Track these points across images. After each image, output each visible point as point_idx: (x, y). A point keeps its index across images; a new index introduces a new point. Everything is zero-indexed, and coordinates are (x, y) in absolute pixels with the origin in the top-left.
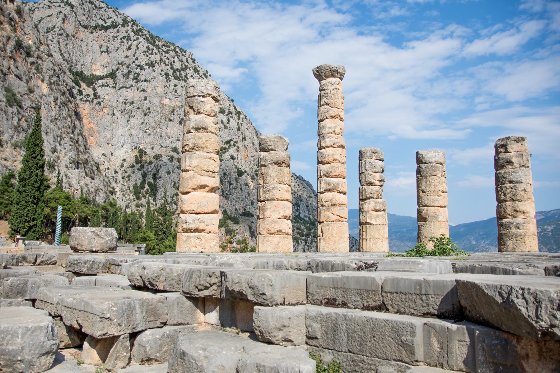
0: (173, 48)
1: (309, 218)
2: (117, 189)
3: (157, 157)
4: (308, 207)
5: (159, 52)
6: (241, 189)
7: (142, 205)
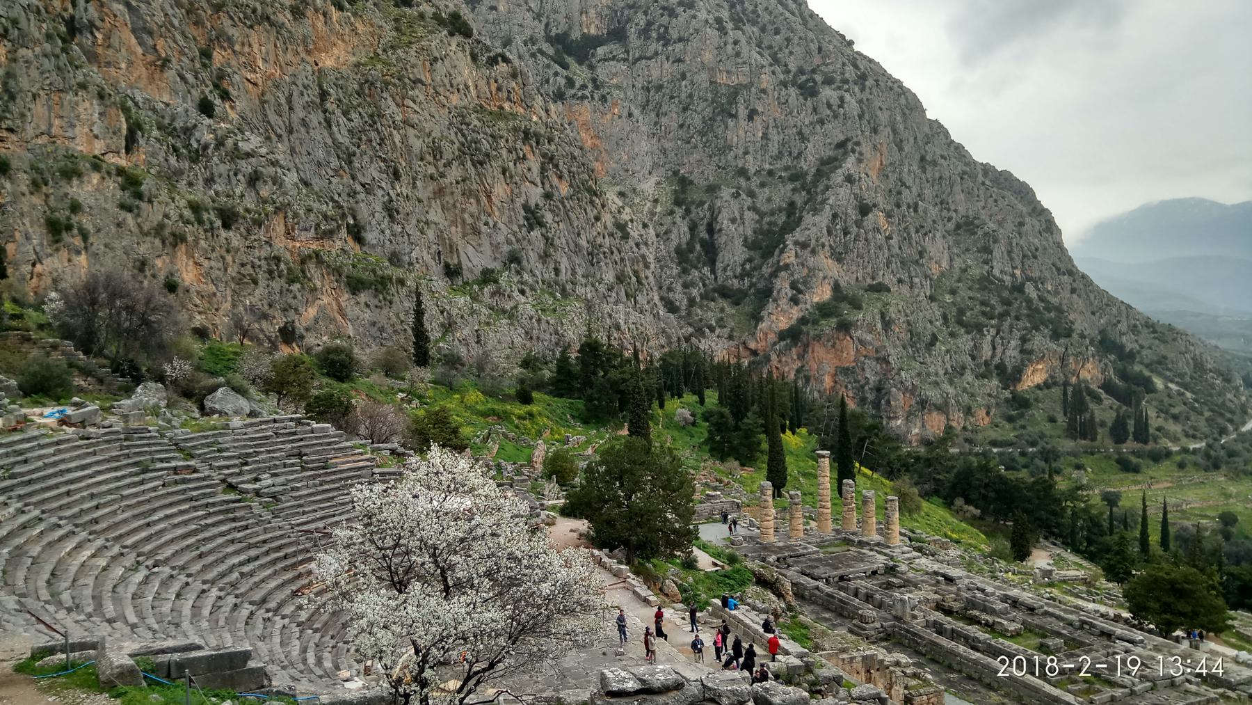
1: (1013, 275)
2: (651, 259)
3: (712, 189)
4: (1010, 252)
6: (866, 240)
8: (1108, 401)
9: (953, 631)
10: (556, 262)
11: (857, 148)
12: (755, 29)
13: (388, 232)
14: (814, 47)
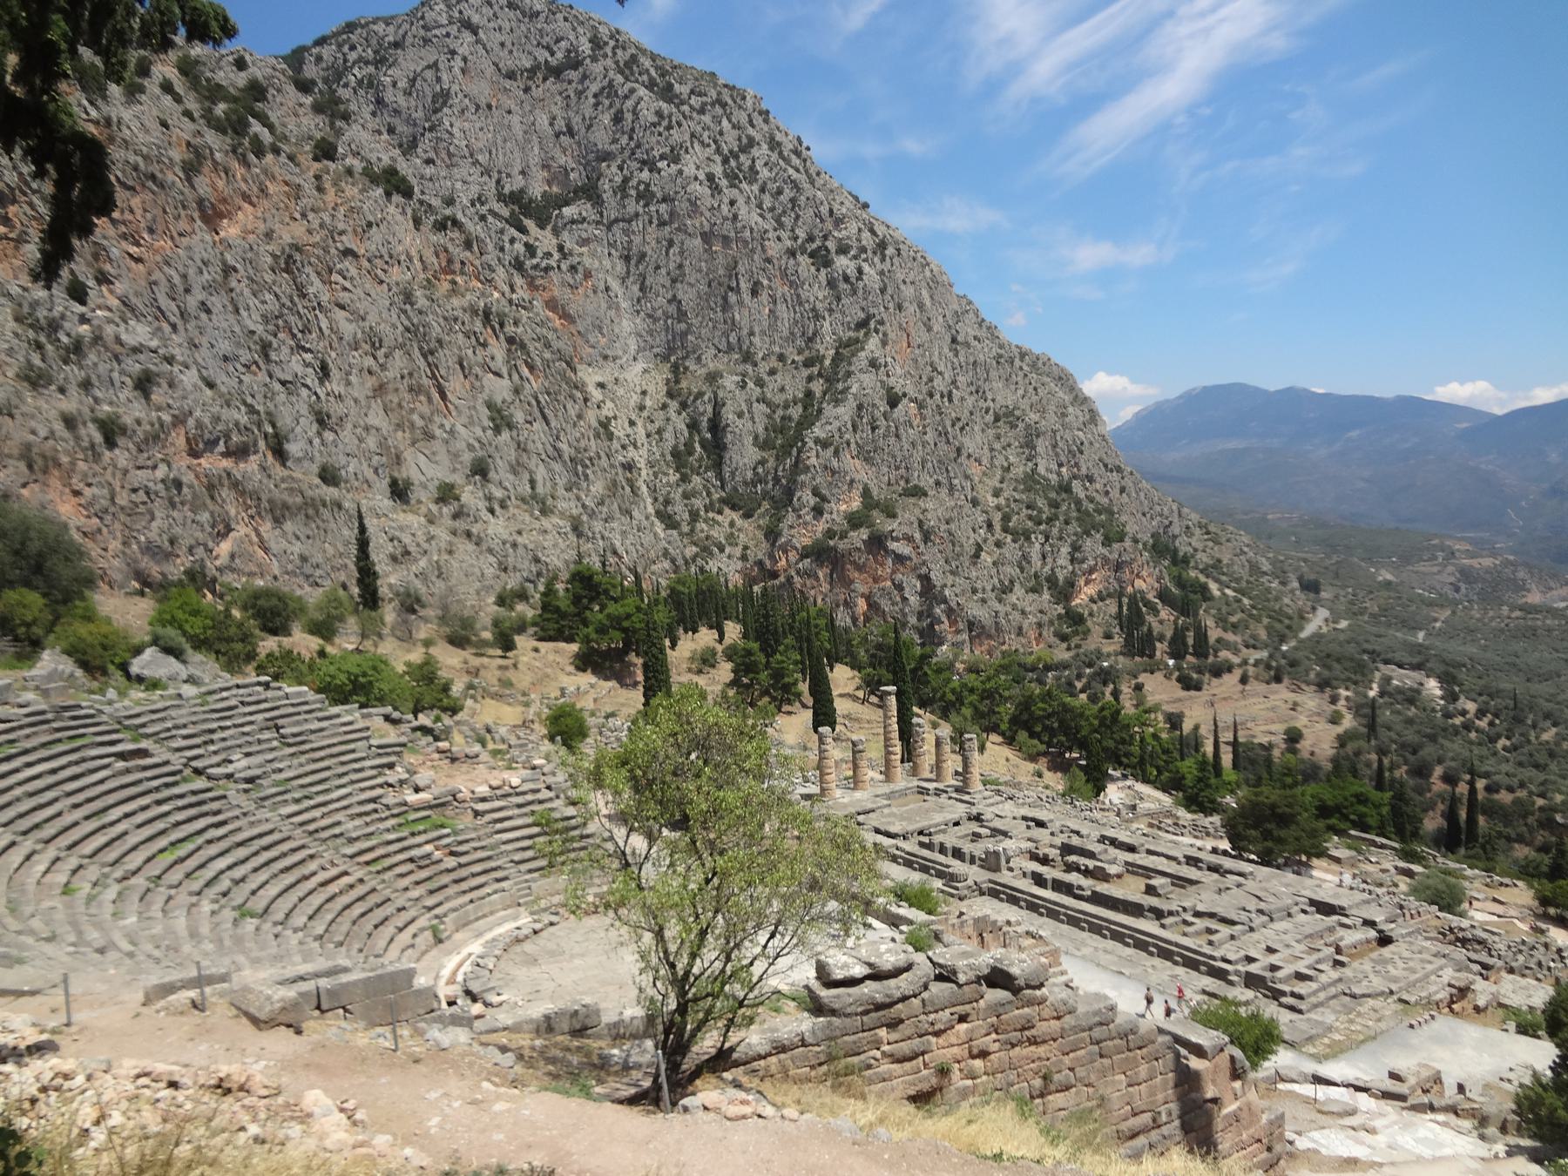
1: (1059, 474)
2: (642, 464)
3: (712, 377)
4: (1055, 446)
8: (1165, 613)
9: (1054, 880)
10: (531, 472)
11: (881, 328)
13: (317, 441)
14: (824, 210)
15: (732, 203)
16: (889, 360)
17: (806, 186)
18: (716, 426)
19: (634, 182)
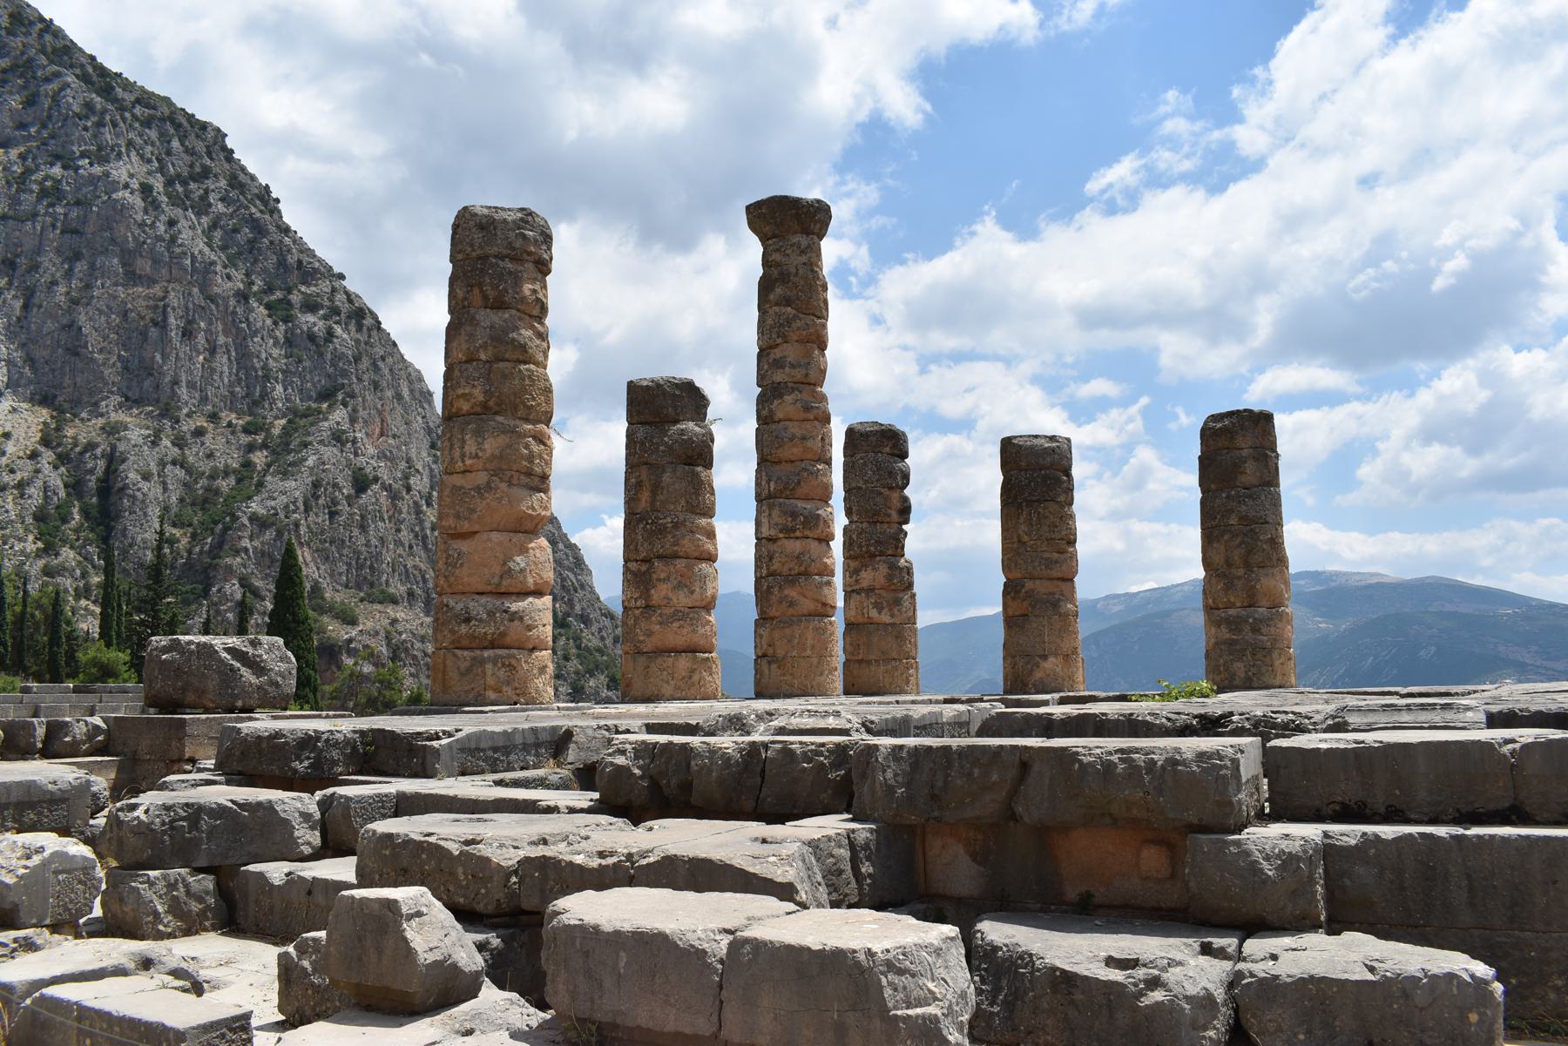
0: (167, 112)
5: (124, 120)
7: (61, 570)
12: (205, 220)
15: (172, 223)
16: (359, 435)
17: (272, 229)
18: (110, 488)
19: (39, 176)
